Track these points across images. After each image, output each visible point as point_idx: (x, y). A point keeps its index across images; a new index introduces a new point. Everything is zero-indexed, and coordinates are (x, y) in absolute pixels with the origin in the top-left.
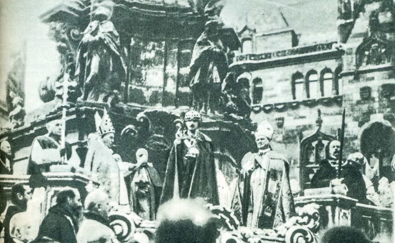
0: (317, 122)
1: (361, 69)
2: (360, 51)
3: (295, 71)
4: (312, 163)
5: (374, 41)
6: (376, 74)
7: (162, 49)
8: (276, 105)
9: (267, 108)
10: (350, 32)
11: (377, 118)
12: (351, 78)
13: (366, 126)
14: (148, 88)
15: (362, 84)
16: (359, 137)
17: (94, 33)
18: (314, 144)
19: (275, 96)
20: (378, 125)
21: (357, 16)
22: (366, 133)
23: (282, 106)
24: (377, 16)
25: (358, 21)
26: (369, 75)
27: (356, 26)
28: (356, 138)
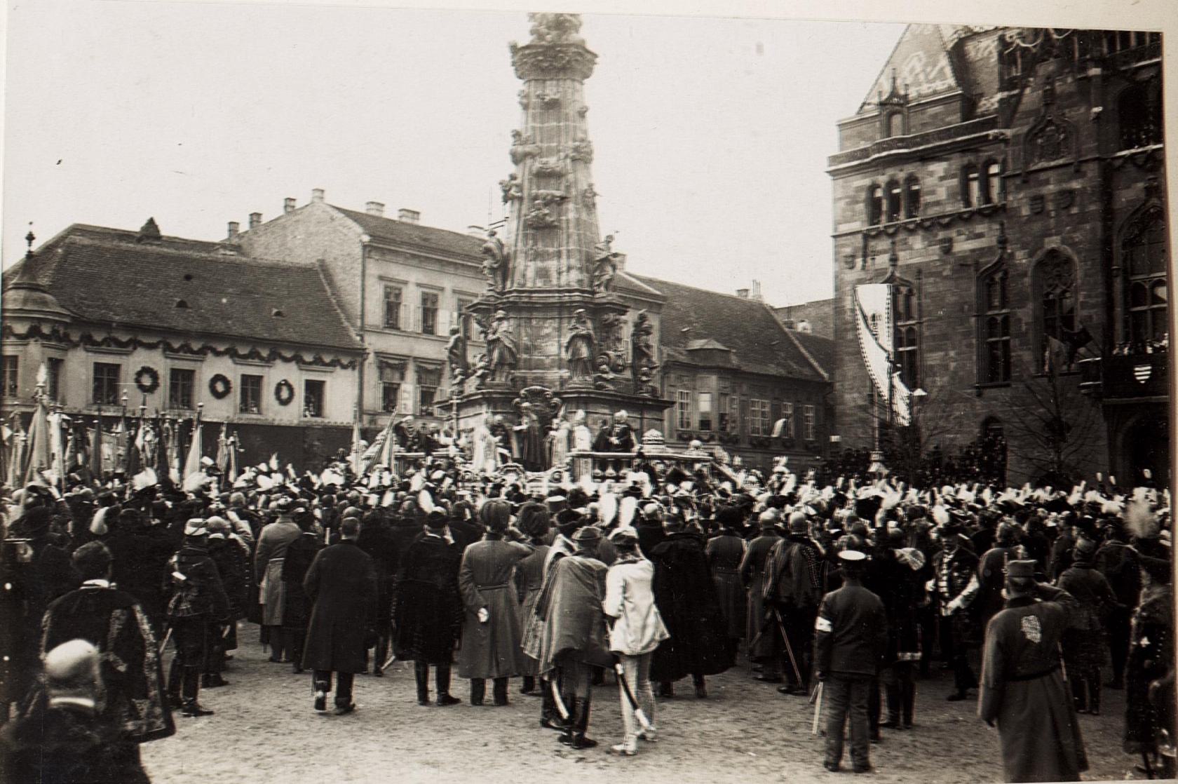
0: (1000, 242)
2: (1032, 135)
4: (995, 308)
5: (1050, 123)
6: (1050, 174)
7: (556, 325)
8: (939, 217)
9: (928, 224)
10: (1015, 111)
11: (1053, 242)
12: (1018, 181)
13: (1040, 254)
15: (1033, 191)
16: (1029, 274)
18: (998, 277)
19: (938, 203)
20: (1053, 253)
22: (1040, 264)
23: (947, 220)
24: (1052, 84)
25: (1028, 91)
26: (1043, 176)
27: (1025, 100)
28: (1025, 275)
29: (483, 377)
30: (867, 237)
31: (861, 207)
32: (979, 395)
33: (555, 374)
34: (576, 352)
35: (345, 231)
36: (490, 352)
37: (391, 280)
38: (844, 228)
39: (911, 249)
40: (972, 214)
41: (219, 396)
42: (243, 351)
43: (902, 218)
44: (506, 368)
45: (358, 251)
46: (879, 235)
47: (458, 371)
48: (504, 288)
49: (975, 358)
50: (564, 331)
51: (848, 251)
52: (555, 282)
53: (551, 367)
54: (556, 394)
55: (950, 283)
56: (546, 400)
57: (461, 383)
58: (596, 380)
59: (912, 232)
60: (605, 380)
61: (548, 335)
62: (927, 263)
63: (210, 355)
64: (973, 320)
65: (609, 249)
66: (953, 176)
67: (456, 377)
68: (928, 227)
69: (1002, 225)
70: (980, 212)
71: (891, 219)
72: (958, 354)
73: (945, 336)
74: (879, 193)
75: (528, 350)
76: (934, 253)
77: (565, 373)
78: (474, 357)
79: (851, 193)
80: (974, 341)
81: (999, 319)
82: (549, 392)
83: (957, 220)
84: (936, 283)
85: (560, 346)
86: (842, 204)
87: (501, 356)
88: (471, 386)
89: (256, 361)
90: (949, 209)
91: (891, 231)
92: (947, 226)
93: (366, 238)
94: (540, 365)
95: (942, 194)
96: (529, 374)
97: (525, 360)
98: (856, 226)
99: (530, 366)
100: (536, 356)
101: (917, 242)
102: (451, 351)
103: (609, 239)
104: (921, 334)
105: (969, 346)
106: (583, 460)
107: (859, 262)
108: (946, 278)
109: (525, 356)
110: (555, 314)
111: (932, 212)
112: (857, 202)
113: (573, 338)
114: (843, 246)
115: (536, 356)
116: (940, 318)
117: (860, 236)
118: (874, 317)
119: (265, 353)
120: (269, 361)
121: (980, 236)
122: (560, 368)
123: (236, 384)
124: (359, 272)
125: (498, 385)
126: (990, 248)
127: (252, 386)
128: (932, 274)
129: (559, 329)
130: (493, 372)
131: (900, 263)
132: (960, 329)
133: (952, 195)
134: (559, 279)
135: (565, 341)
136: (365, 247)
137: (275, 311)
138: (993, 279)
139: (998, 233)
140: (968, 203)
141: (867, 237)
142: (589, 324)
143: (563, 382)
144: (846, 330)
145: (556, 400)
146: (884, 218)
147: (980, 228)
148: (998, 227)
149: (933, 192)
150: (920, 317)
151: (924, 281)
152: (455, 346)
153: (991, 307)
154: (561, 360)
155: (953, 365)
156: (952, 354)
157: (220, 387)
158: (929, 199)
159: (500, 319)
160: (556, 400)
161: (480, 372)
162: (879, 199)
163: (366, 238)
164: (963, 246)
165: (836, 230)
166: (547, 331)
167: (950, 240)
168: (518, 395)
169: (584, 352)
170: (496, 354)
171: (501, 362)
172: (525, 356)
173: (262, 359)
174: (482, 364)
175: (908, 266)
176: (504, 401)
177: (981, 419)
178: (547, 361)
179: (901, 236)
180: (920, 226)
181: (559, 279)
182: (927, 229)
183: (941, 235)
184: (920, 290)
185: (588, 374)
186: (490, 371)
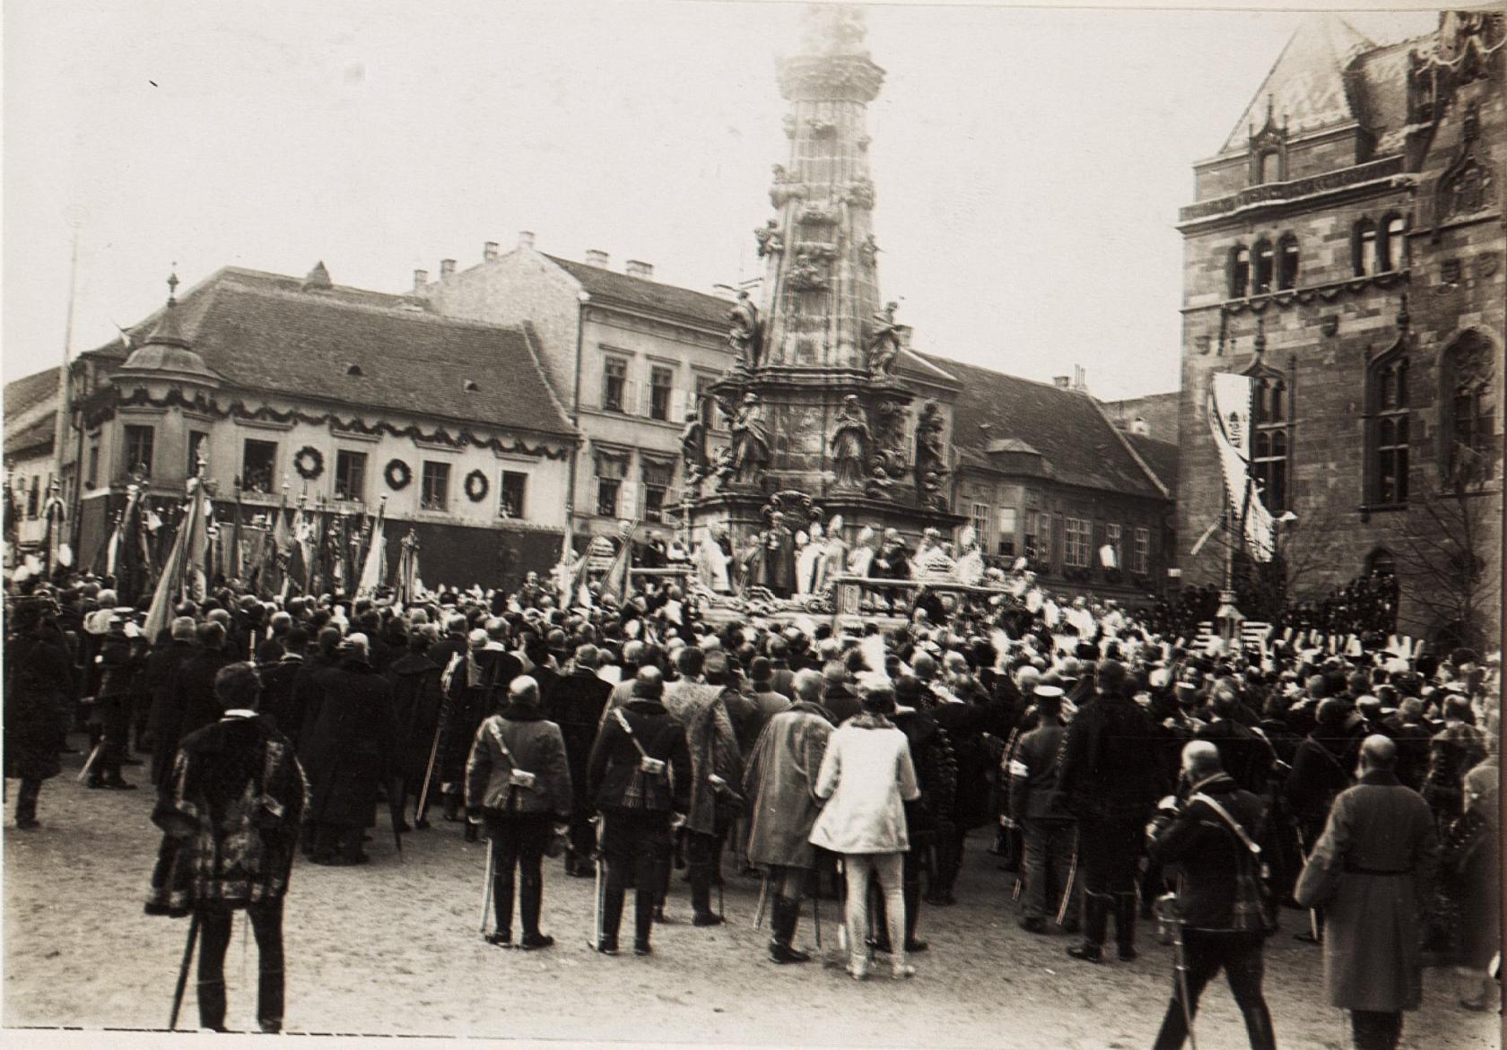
0: (1400, 321)
1: (1447, 223)
3: (1359, 215)
5: (1472, 164)
8: (1322, 289)
9: (1307, 297)
10: (1426, 149)
12: (1427, 241)
14: (808, 453)
17: (741, 422)
18: (1395, 367)
19: (1320, 270)
21: (1440, 116)
23: (1332, 292)
24: (1476, 113)
25: (1444, 123)
27: (1440, 134)
28: (1431, 363)
29: (725, 477)
30: (1226, 313)
31: (1220, 274)
32: (1365, 520)
33: (816, 477)
34: (844, 449)
35: (559, 286)
36: (736, 445)
37: (614, 350)
38: (1196, 301)
39: (1284, 329)
40: (1366, 284)
41: (396, 486)
42: (428, 431)
43: (1274, 288)
44: (755, 466)
45: (574, 312)
46: (1242, 310)
47: (694, 467)
48: (756, 364)
49: (1361, 472)
50: (830, 422)
51: (1199, 331)
52: (821, 359)
53: (812, 467)
54: (817, 502)
55: (1333, 376)
56: (804, 510)
57: (698, 483)
58: (868, 485)
59: (1286, 308)
60: (883, 488)
61: (809, 427)
62: (1305, 348)
63: (387, 436)
64: (1361, 422)
65: (891, 319)
66: (1342, 236)
67: (690, 475)
68: (1308, 300)
69: (1404, 298)
70: (1375, 282)
71: (1258, 290)
72: (1339, 467)
73: (1324, 444)
74: (1244, 256)
75: (783, 444)
76: (1313, 336)
77: (829, 476)
78: (715, 451)
79: (1208, 256)
80: (1361, 450)
81: (1395, 421)
82: (808, 498)
83: (1346, 292)
84: (1314, 373)
85: (824, 441)
86: (1196, 270)
87: (749, 450)
88: (710, 487)
89: (444, 445)
90: (1335, 278)
91: (1258, 305)
92: (1331, 301)
93: (585, 296)
94: (799, 465)
95: (1327, 258)
96: (784, 475)
97: (780, 457)
98: (1214, 298)
99: (785, 464)
100: (794, 453)
101: (1292, 321)
102: (686, 443)
103: (892, 308)
104: (1292, 439)
105: (1355, 455)
106: (847, 587)
107: (1215, 345)
108: (1329, 367)
109: (779, 452)
110: (820, 400)
111: (1312, 282)
112: (1216, 268)
113: (841, 432)
114: (1194, 324)
115: (794, 453)
116: (1318, 420)
117: (1217, 313)
118: (1234, 417)
119: (454, 435)
120: (458, 446)
121: (1375, 313)
122: (823, 469)
123: (418, 472)
124: (574, 338)
125: (744, 487)
126: (1387, 330)
127: (436, 476)
128: (1309, 363)
129: (824, 420)
130: (738, 472)
131: (1267, 348)
132: (1344, 434)
133: (1339, 260)
134: (826, 355)
135: (830, 435)
136: (582, 306)
137: (468, 383)
138: (1388, 370)
139: (1398, 309)
140: (1360, 271)
141: (1226, 313)
142: (863, 415)
143: (826, 487)
144: (1195, 433)
145: (817, 509)
146: (1249, 289)
147: (1373, 303)
148: (1399, 301)
149: (1315, 256)
150: (1293, 417)
151: (1299, 371)
152: (692, 436)
153: (1385, 406)
154: (825, 458)
155: (1332, 481)
156: (1332, 466)
157: (398, 475)
158: (1309, 265)
159: (750, 405)
160: (817, 509)
161: (721, 470)
162: (1245, 265)
163: (585, 296)
164: (1351, 326)
165: (1186, 303)
166: (808, 421)
167: (1335, 319)
168: (769, 502)
169: (855, 449)
170: (742, 449)
171: (749, 459)
172: (779, 452)
173: (449, 442)
174: (725, 460)
175: (1279, 352)
176: (748, 509)
177: (1368, 551)
178: (807, 460)
179: (1270, 313)
180: (1296, 300)
181: (826, 355)
182: (1305, 304)
183: (1324, 311)
184: (1293, 382)
185: (859, 478)
186: (734, 469)
